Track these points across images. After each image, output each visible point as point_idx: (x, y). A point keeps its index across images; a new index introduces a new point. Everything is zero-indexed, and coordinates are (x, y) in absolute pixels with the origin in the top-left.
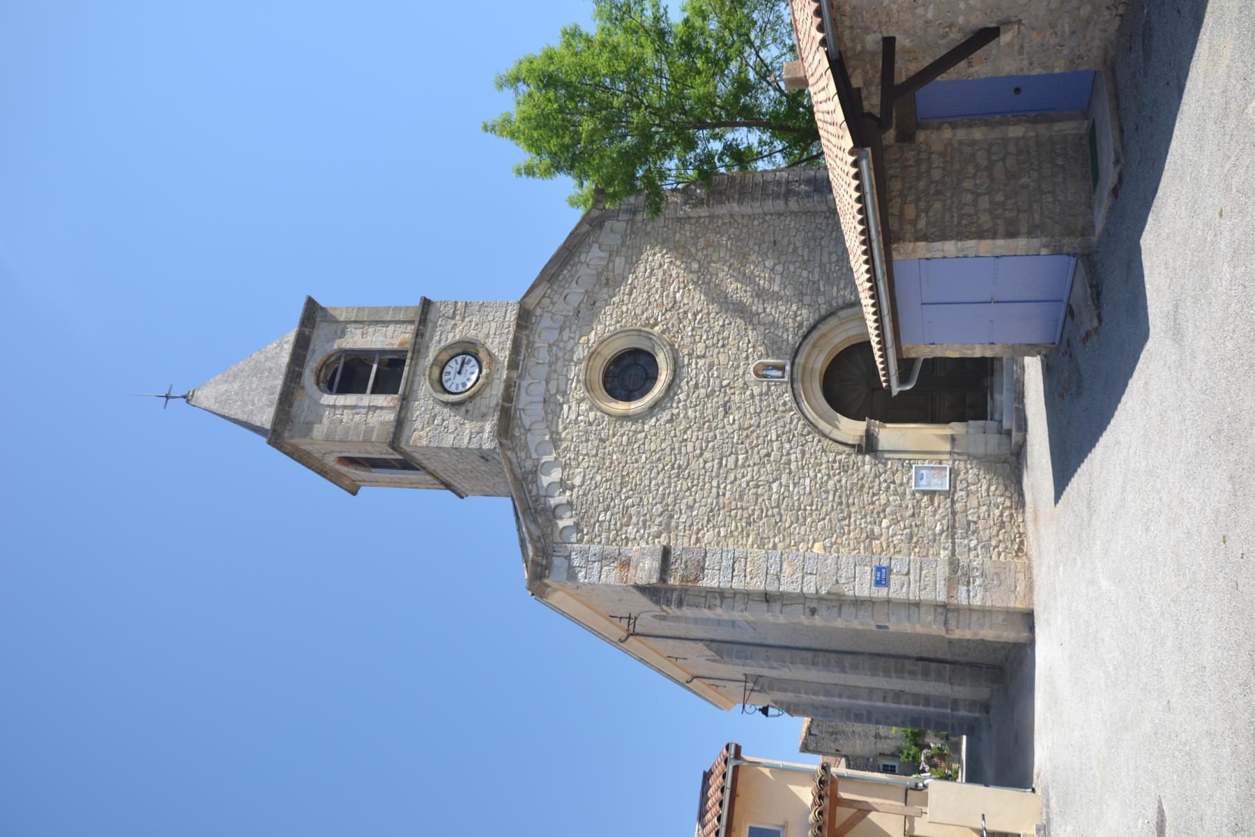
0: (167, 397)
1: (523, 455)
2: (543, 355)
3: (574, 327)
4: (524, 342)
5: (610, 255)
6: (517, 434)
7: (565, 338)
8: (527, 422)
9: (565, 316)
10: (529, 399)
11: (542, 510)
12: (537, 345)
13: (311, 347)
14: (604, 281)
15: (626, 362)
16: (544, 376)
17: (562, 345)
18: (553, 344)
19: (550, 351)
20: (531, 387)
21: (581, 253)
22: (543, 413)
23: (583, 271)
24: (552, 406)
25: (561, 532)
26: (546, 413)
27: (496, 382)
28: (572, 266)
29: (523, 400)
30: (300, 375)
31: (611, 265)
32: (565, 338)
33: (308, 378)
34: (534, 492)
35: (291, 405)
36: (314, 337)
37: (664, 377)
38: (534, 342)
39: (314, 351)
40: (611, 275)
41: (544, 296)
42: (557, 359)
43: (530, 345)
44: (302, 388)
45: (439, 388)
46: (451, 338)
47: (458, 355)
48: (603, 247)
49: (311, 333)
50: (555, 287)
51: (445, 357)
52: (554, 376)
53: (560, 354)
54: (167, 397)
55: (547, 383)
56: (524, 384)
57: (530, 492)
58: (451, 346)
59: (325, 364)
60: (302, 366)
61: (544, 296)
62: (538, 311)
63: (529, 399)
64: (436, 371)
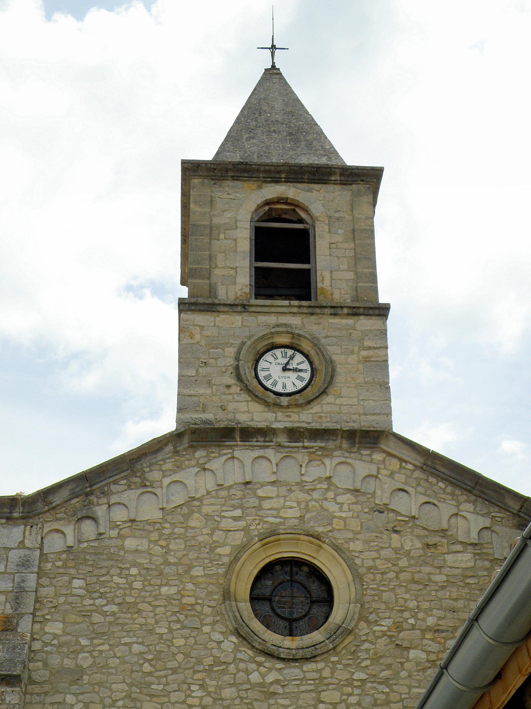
0: (273, 47)
1: (168, 466)
2: (315, 472)
3: (358, 507)
4: (331, 445)
5: (474, 545)
6: (198, 454)
7: (340, 499)
8: (216, 464)
9: (374, 494)
10: (248, 462)
11: (91, 503)
12: (327, 461)
13: (316, 186)
14: (432, 540)
15: (314, 586)
16: (282, 477)
17: (330, 495)
18: (330, 484)
19: (320, 480)
20: (265, 463)
21: (474, 502)
22: (227, 484)
23: (446, 509)
24: (239, 494)
25: (58, 531)
26: (230, 487)
27: (270, 416)
28: (453, 494)
29: (246, 454)
30: (277, 181)
31: (459, 548)
32: (340, 499)
33: (273, 191)
34: (114, 488)
35: (234, 178)
36: (331, 187)
37: (272, 638)
38: (330, 456)
39: (310, 191)
40: (441, 550)
41: (401, 460)
42: (309, 492)
43: (327, 453)
44: (260, 187)
45: (261, 346)
46: (335, 352)
47: (311, 363)
48: (486, 534)
49: (335, 183)
50: (417, 474)
51: (306, 346)
52: (283, 490)
53: (316, 495)
54: (273, 47)
55: (273, 483)
56: (270, 453)
57: (115, 483)
58: (320, 351)
59: (295, 205)
60: (288, 181)
61: (401, 460)
62: (378, 457)
63: (248, 462)
64: (285, 340)
